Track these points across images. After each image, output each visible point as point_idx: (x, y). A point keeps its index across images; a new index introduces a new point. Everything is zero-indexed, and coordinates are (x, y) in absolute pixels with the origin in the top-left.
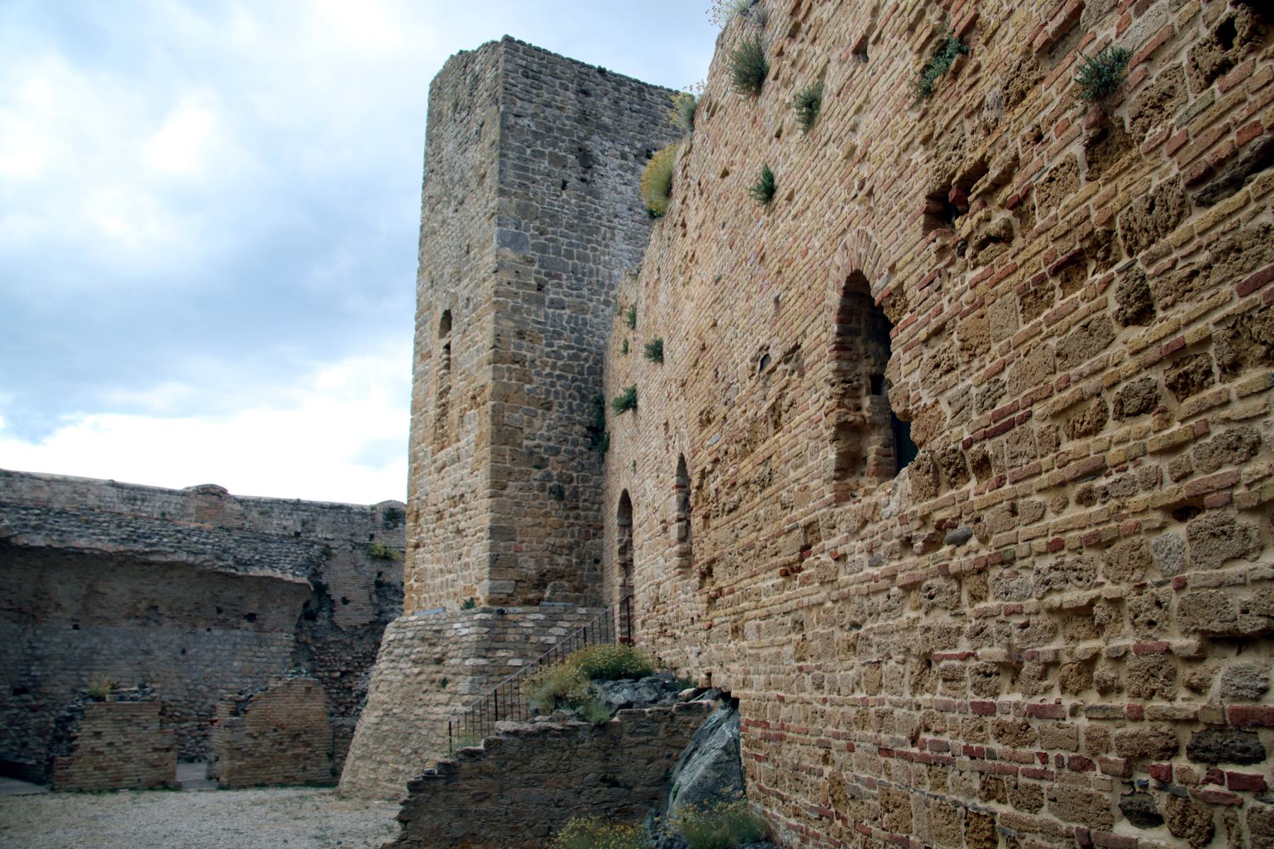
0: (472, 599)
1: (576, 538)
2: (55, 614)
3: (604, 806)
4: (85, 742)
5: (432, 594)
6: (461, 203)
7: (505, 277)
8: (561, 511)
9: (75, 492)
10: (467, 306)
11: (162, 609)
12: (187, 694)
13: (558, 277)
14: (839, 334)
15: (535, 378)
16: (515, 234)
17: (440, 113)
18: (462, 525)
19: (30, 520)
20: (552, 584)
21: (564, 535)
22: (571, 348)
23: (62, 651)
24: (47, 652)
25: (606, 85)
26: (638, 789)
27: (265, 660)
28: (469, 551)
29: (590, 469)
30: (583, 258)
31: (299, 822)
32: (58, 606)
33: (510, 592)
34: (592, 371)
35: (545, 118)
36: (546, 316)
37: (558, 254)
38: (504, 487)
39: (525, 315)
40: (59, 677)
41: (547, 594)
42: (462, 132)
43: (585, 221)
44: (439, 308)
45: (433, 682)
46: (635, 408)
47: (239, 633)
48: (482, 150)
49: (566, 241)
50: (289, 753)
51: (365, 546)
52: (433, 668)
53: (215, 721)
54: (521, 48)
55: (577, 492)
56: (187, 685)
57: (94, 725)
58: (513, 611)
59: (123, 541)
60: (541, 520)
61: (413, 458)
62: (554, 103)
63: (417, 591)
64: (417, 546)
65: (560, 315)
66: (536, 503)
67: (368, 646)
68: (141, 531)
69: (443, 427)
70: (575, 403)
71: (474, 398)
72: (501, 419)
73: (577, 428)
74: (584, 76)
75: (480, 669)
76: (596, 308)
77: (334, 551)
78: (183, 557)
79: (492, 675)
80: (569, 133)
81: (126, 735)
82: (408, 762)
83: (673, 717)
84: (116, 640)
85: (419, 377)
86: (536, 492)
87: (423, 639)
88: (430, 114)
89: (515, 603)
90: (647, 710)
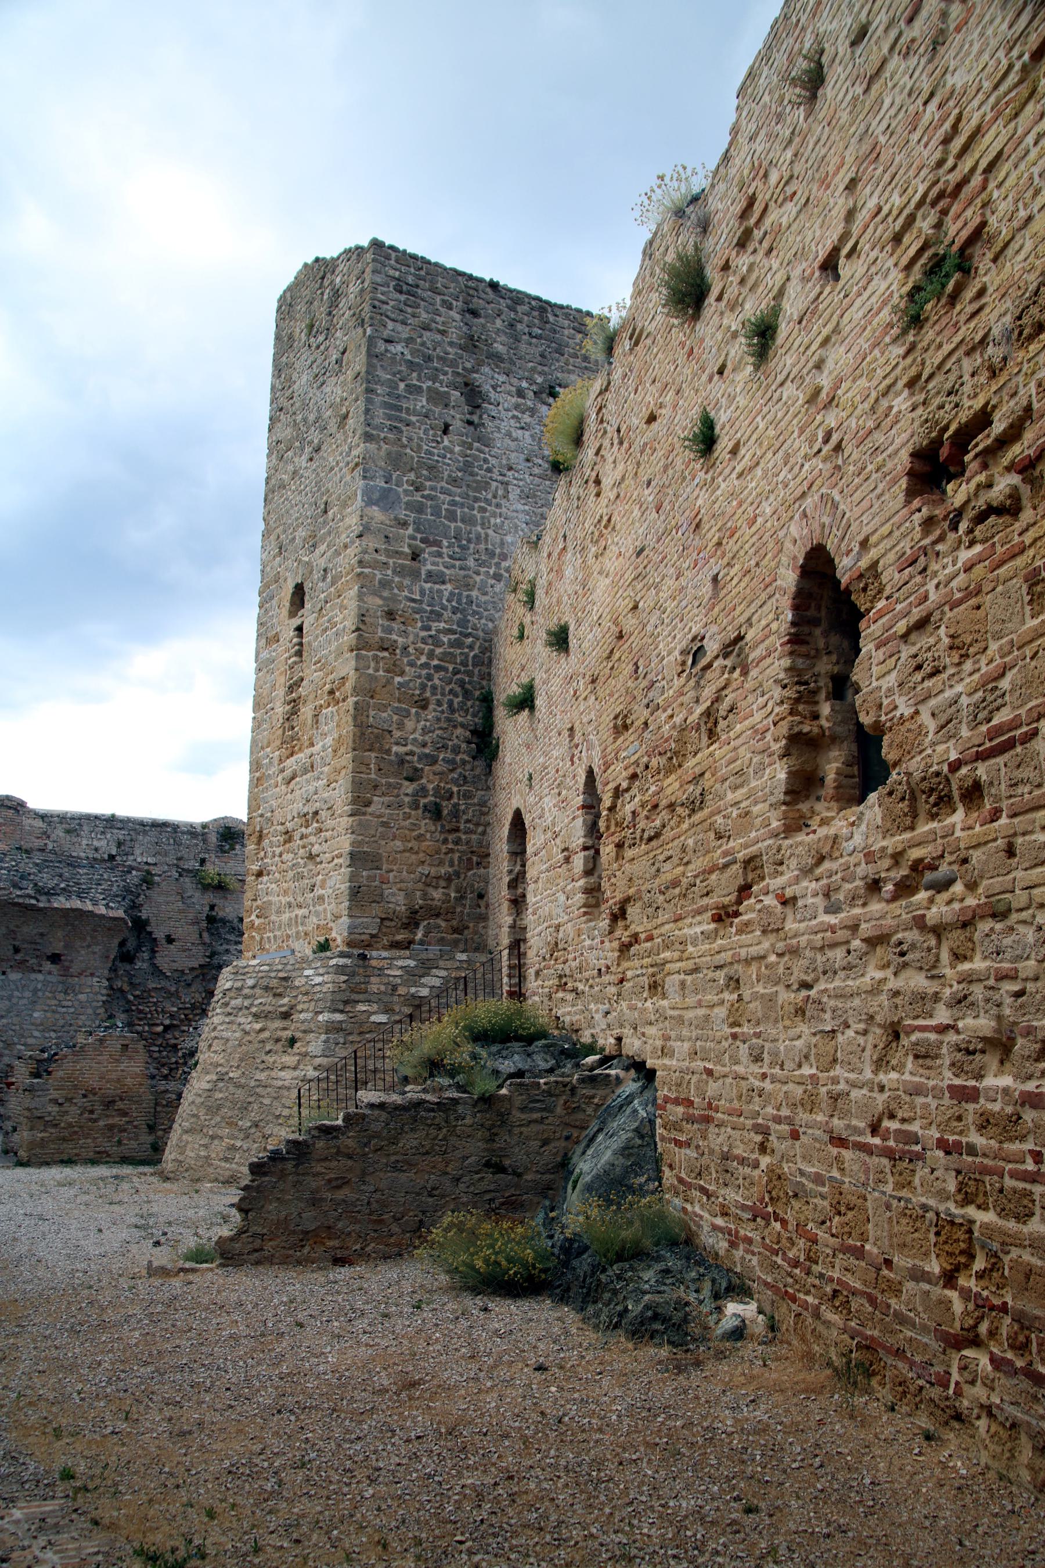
0: (327, 940)
3: (488, 1197)
5: (278, 933)
6: (317, 450)
7: (372, 542)
8: (437, 834)
10: (324, 579)
13: (438, 544)
14: (793, 624)
15: (407, 669)
16: (385, 489)
17: (291, 337)
18: (316, 849)
21: (441, 863)
22: (454, 632)
25: (499, 304)
26: (528, 1177)
27: (72, 1010)
28: (324, 881)
30: (469, 521)
31: (116, 1208)
33: (374, 932)
34: (478, 661)
35: (423, 344)
36: (422, 592)
37: (436, 512)
38: (368, 804)
39: (396, 591)
41: (419, 935)
42: (319, 361)
43: (472, 474)
44: (289, 580)
45: (278, 1040)
46: (532, 708)
47: (40, 977)
48: (344, 384)
49: (448, 498)
51: (194, 873)
52: (278, 1024)
53: (13, 1084)
54: (393, 255)
55: (457, 811)
58: (378, 955)
60: (413, 844)
61: (256, 766)
63: (259, 929)
64: (260, 874)
65: (440, 591)
67: (197, 995)
69: (293, 728)
70: (456, 701)
71: (331, 692)
72: (364, 719)
73: (459, 731)
74: (471, 292)
75: (337, 1025)
80: (453, 364)
83: (573, 1090)
85: (263, 666)
86: (407, 810)
87: (267, 988)
88: (278, 338)
89: (379, 945)
90: (542, 1081)
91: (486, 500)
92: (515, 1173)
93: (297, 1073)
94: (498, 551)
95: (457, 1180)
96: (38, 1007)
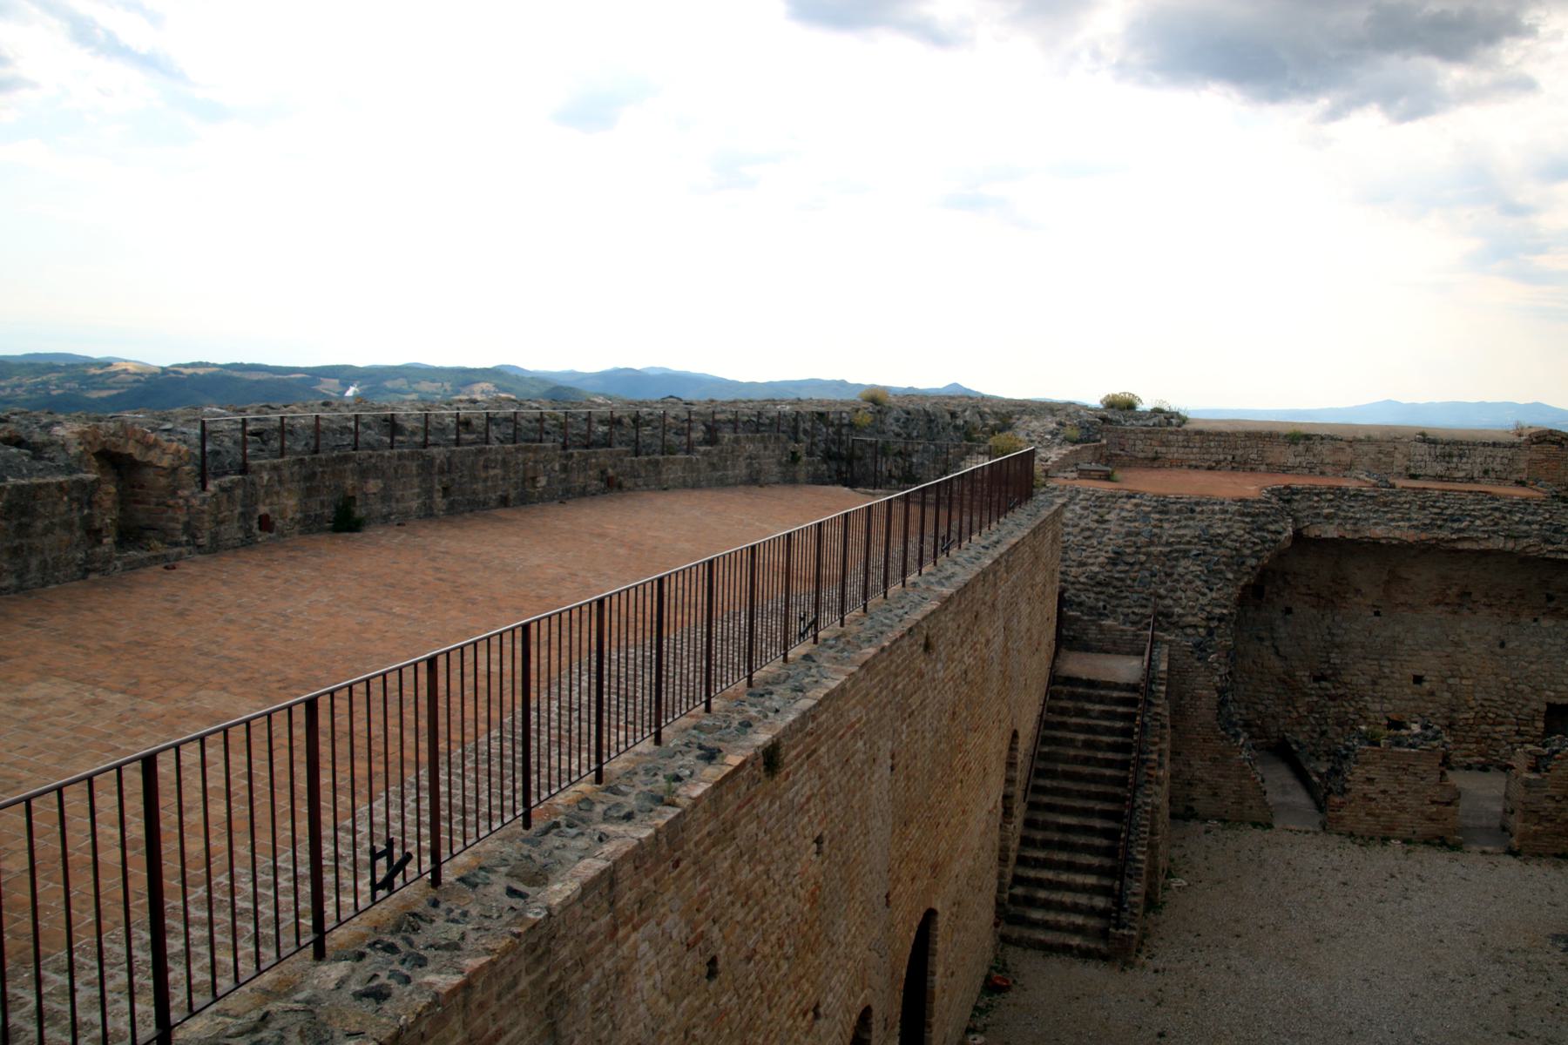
4: (1358, 788)
9: (1380, 452)
19: (1322, 508)
24: (1346, 639)
32: (1358, 591)
40: (1359, 666)
56: (1505, 683)
57: (1368, 771)
68: (1449, 512)
78: (1498, 543)
81: (1401, 784)
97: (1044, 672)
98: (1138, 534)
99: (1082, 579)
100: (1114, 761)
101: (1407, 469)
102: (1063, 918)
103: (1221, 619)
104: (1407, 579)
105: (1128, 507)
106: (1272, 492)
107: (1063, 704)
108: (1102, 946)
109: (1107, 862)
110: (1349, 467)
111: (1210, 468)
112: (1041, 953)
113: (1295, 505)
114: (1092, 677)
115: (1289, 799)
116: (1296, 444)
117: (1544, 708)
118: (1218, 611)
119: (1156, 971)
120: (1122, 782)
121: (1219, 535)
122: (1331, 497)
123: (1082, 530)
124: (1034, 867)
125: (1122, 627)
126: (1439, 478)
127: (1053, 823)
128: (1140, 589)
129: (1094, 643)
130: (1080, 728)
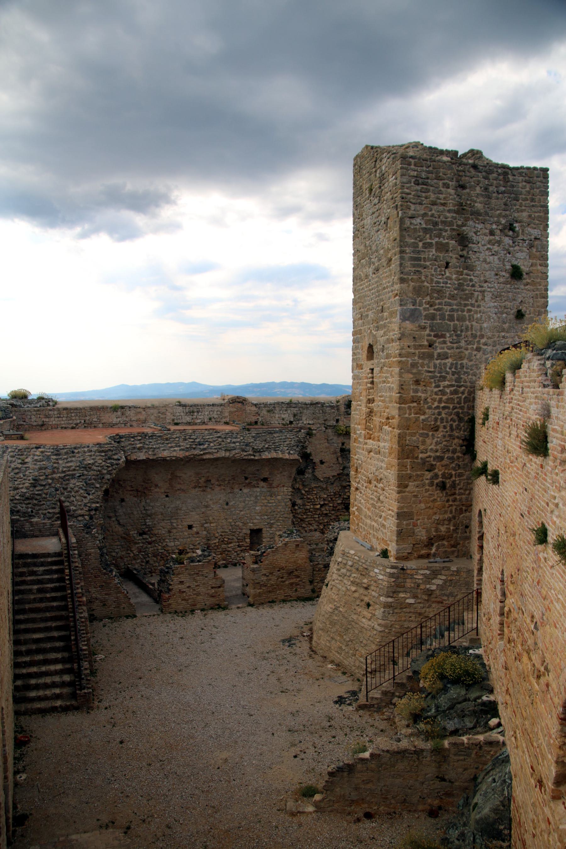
1: (454, 514)
2: (156, 490)
3: (437, 791)
4: (176, 587)
7: (407, 342)
8: (444, 498)
9: (159, 413)
11: (213, 481)
12: (230, 528)
13: (443, 336)
15: (427, 411)
16: (412, 310)
19: (136, 444)
20: (437, 544)
21: (446, 512)
23: (161, 510)
24: (153, 511)
25: (478, 176)
26: (457, 784)
27: (275, 504)
29: (464, 468)
30: (461, 319)
32: (156, 486)
33: (410, 551)
34: (467, 400)
36: (435, 366)
37: (443, 318)
38: (406, 486)
39: (420, 368)
40: (161, 524)
41: (434, 550)
43: (463, 290)
45: (362, 600)
47: (258, 490)
49: (449, 308)
50: (287, 582)
51: (334, 427)
52: (362, 591)
55: (455, 484)
56: (230, 523)
59: (187, 449)
62: (439, 201)
64: (357, 489)
65: (445, 364)
66: (427, 494)
67: (337, 488)
68: (197, 440)
70: (454, 424)
73: (456, 441)
74: (461, 174)
75: (389, 604)
76: (470, 355)
77: (314, 432)
78: (222, 454)
79: (396, 608)
81: (197, 582)
82: (347, 645)
83: (481, 748)
84: (189, 501)
86: (427, 487)
87: (357, 569)
89: (412, 557)
91: (472, 305)
92: (450, 781)
93: (370, 623)
94: (478, 333)
95: (423, 783)
96: (258, 504)
97: (10, 553)
98: (46, 468)
99: (17, 497)
100: (56, 597)
101: (173, 420)
102: (48, 692)
103: (96, 509)
104: (180, 477)
105: (38, 453)
106: (110, 438)
107: (21, 570)
108: (73, 702)
109: (66, 655)
110: (145, 421)
111: (73, 428)
112: (40, 716)
113: (122, 444)
114: (34, 552)
115: (139, 600)
116: (117, 411)
117: (249, 532)
118: (94, 505)
119: (106, 708)
120: (65, 608)
121: (90, 464)
122: (140, 438)
123: (13, 469)
124: (24, 667)
125: (43, 521)
126: (189, 424)
127: (30, 639)
128: (50, 499)
129: (29, 533)
130: (33, 582)
